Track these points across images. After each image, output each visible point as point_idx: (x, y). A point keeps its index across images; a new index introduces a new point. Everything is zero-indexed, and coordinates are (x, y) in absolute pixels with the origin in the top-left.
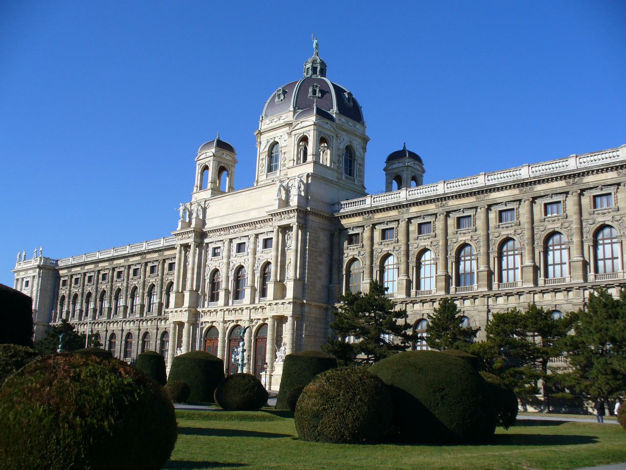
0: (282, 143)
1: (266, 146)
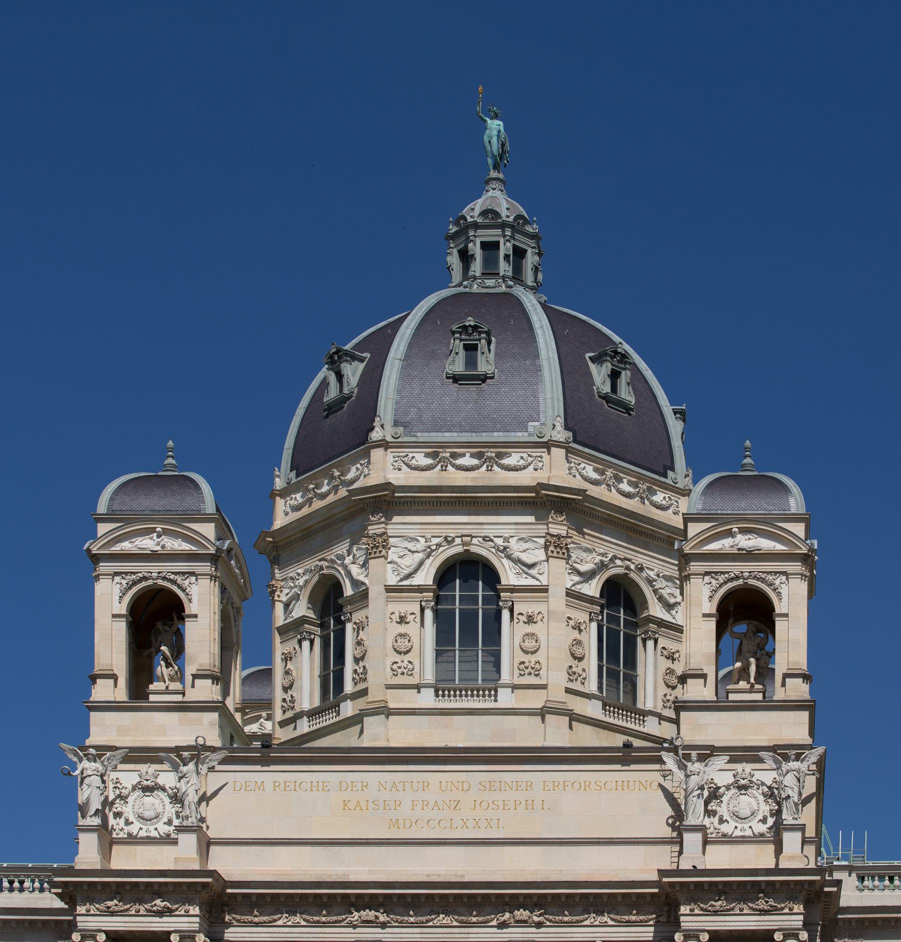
0: (509, 576)
1: (421, 564)
